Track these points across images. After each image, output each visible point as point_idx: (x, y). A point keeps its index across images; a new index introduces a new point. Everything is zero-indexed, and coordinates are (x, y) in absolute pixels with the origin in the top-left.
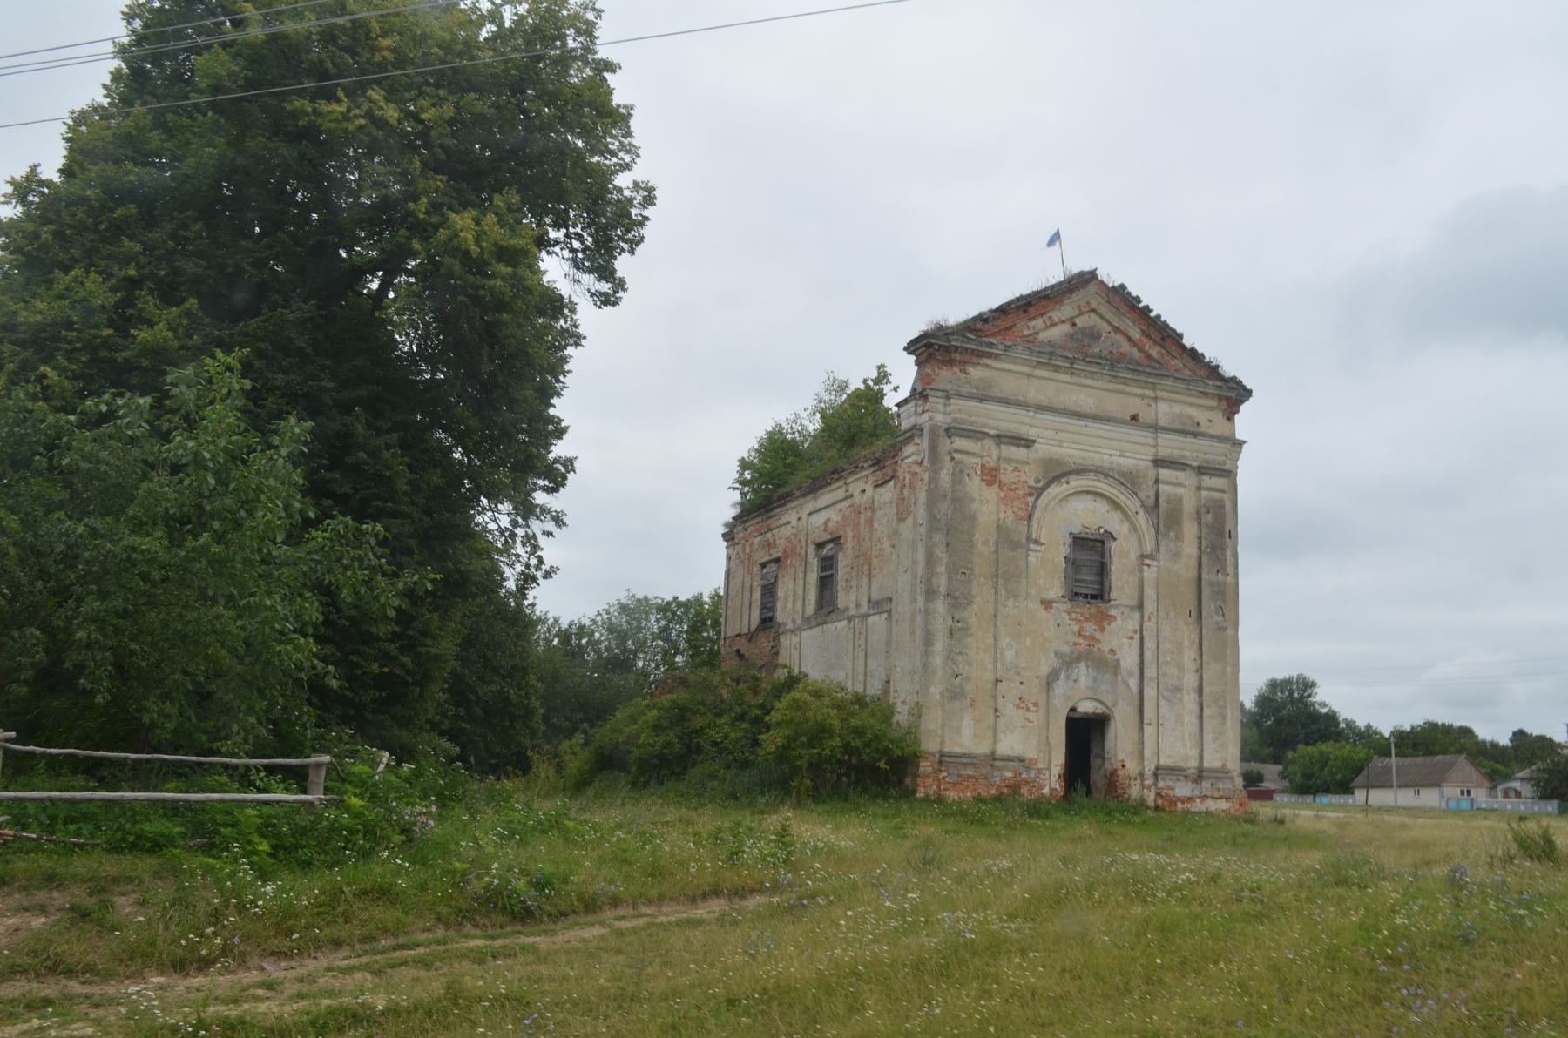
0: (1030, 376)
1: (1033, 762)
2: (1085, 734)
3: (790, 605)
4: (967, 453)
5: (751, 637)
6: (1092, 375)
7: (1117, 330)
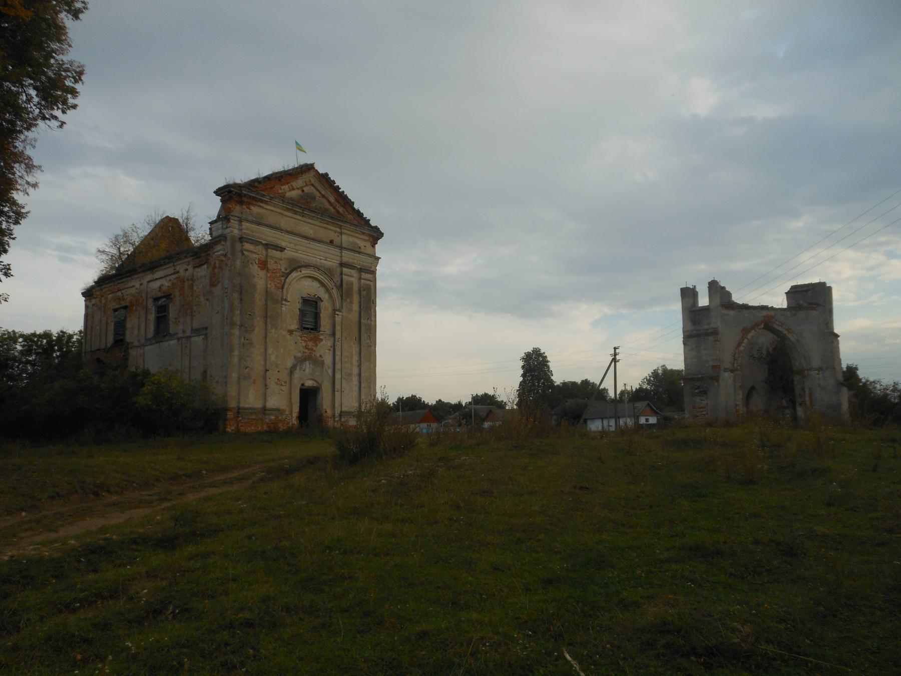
1: (284, 411)
2: (308, 396)
3: (136, 332)
4: (251, 252)
5: (108, 350)
6: (312, 218)
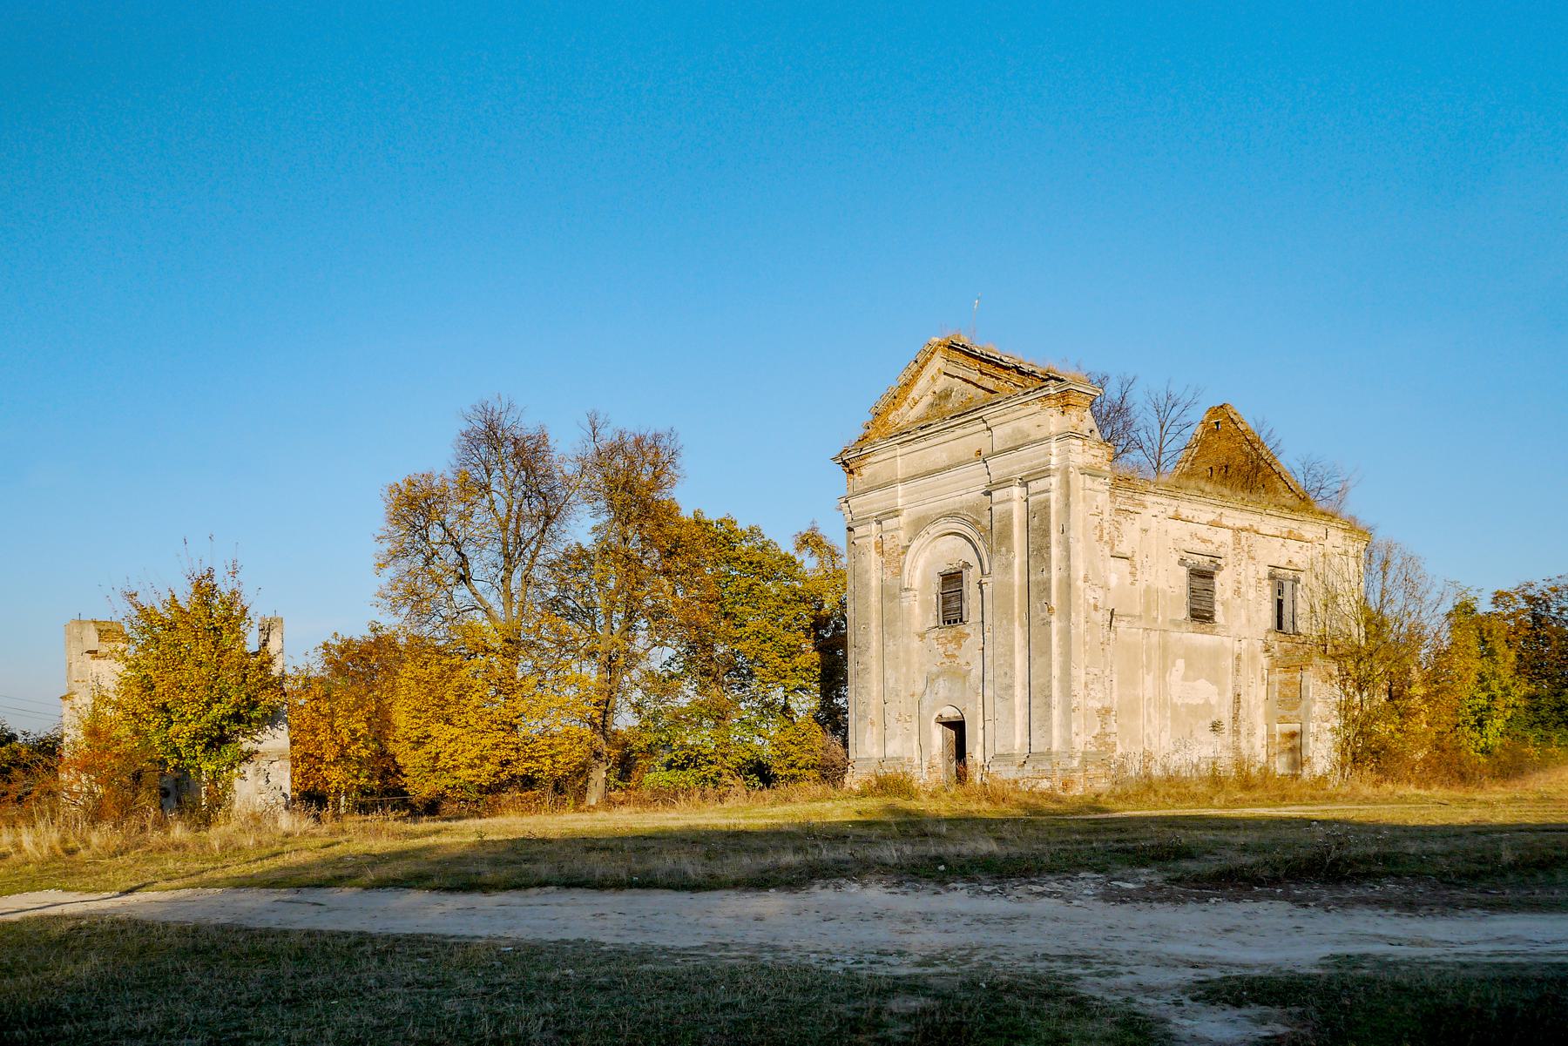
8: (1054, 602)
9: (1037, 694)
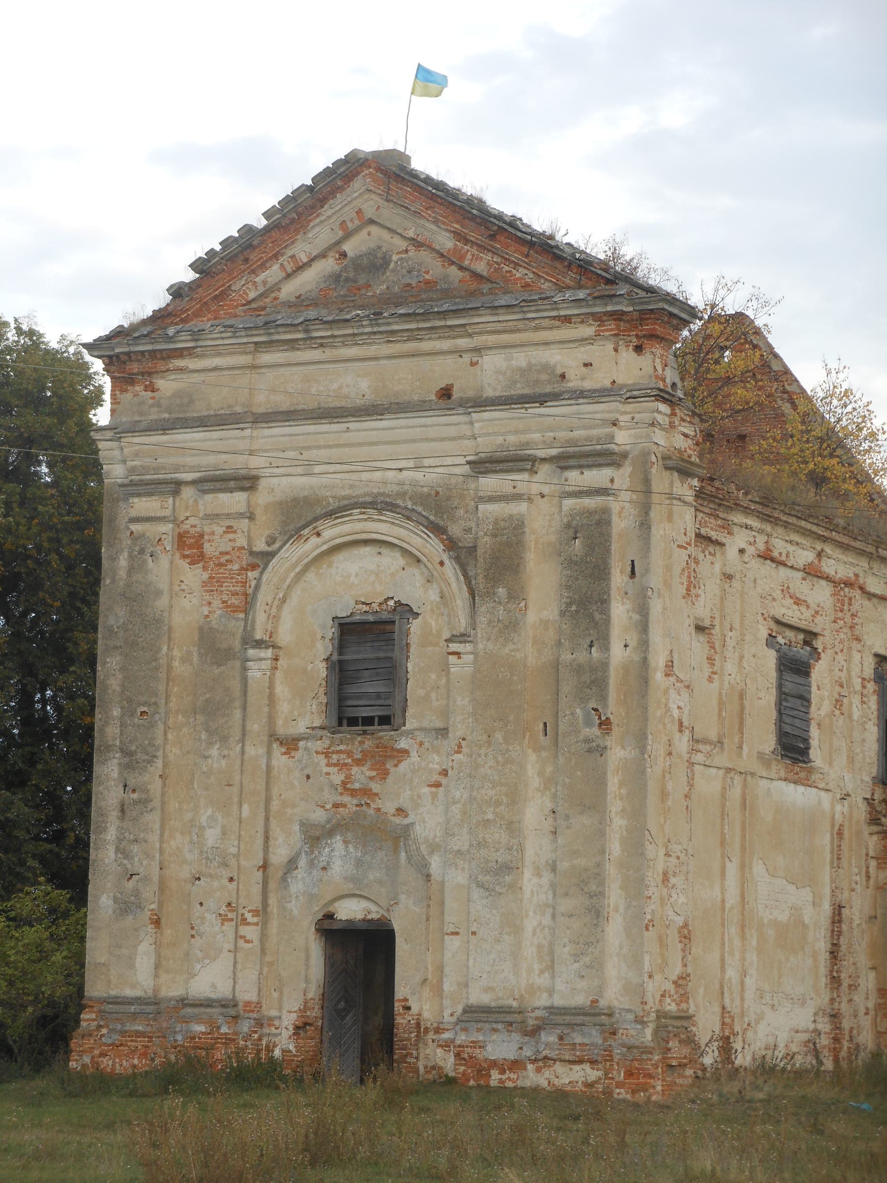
0: (254, 367)
2: (362, 956)
6: (352, 339)
7: (418, 244)
8: (614, 709)
9: (584, 891)
